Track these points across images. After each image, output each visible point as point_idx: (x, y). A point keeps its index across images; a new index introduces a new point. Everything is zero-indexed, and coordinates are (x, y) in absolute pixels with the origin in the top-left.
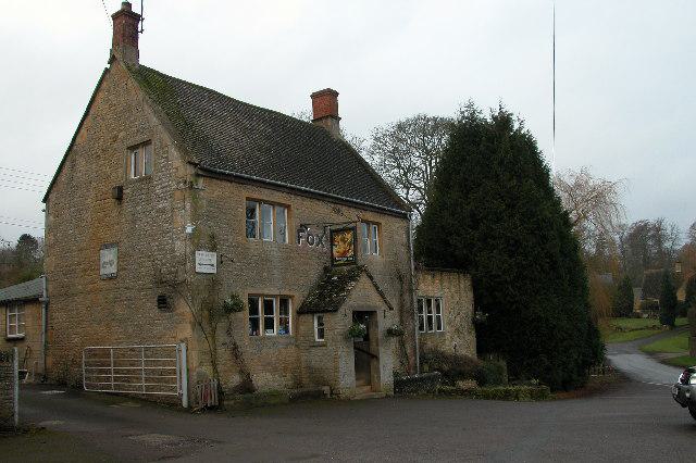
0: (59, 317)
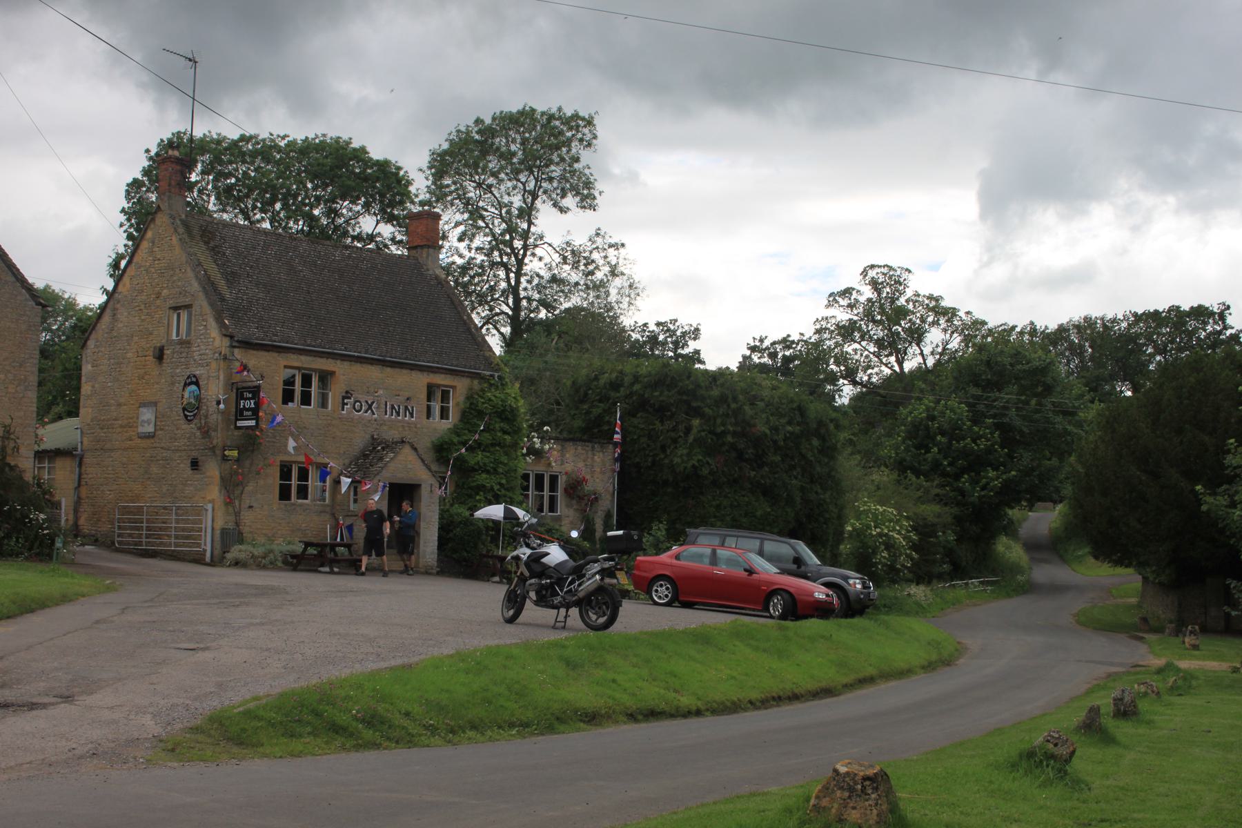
0: (91, 471)
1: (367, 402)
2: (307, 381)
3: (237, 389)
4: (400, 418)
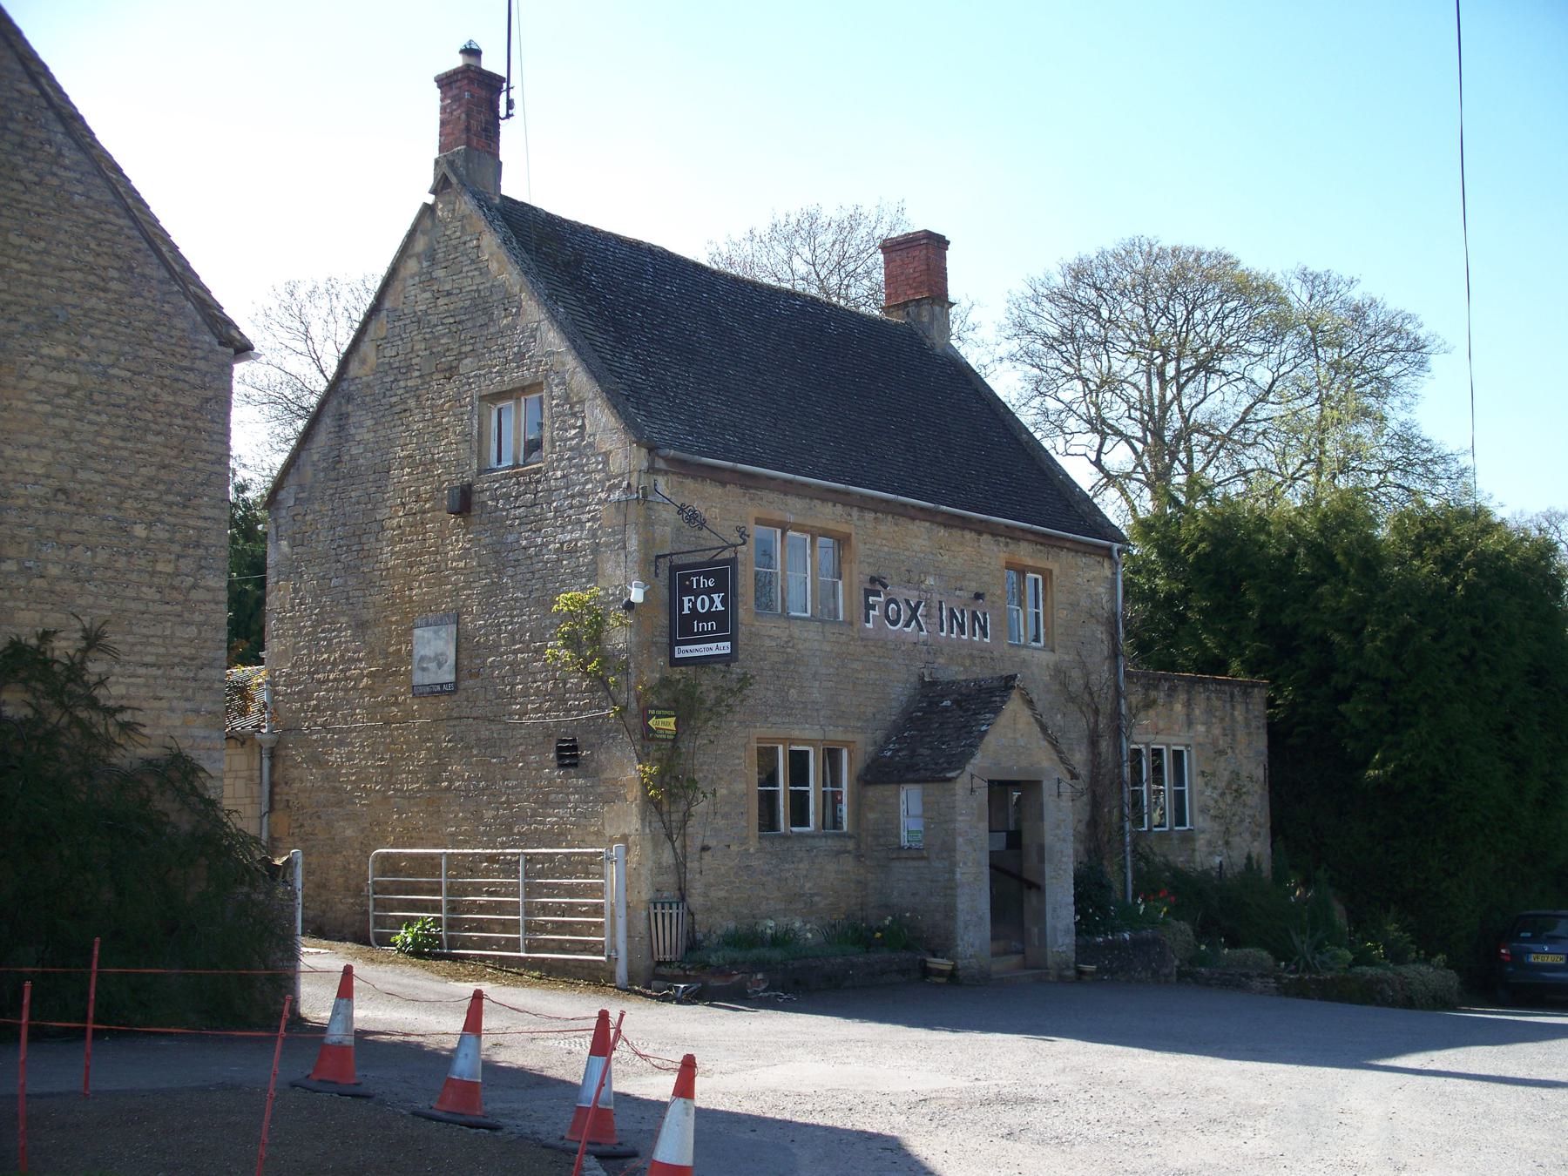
1: (907, 602)
3: (673, 569)
4: (965, 637)
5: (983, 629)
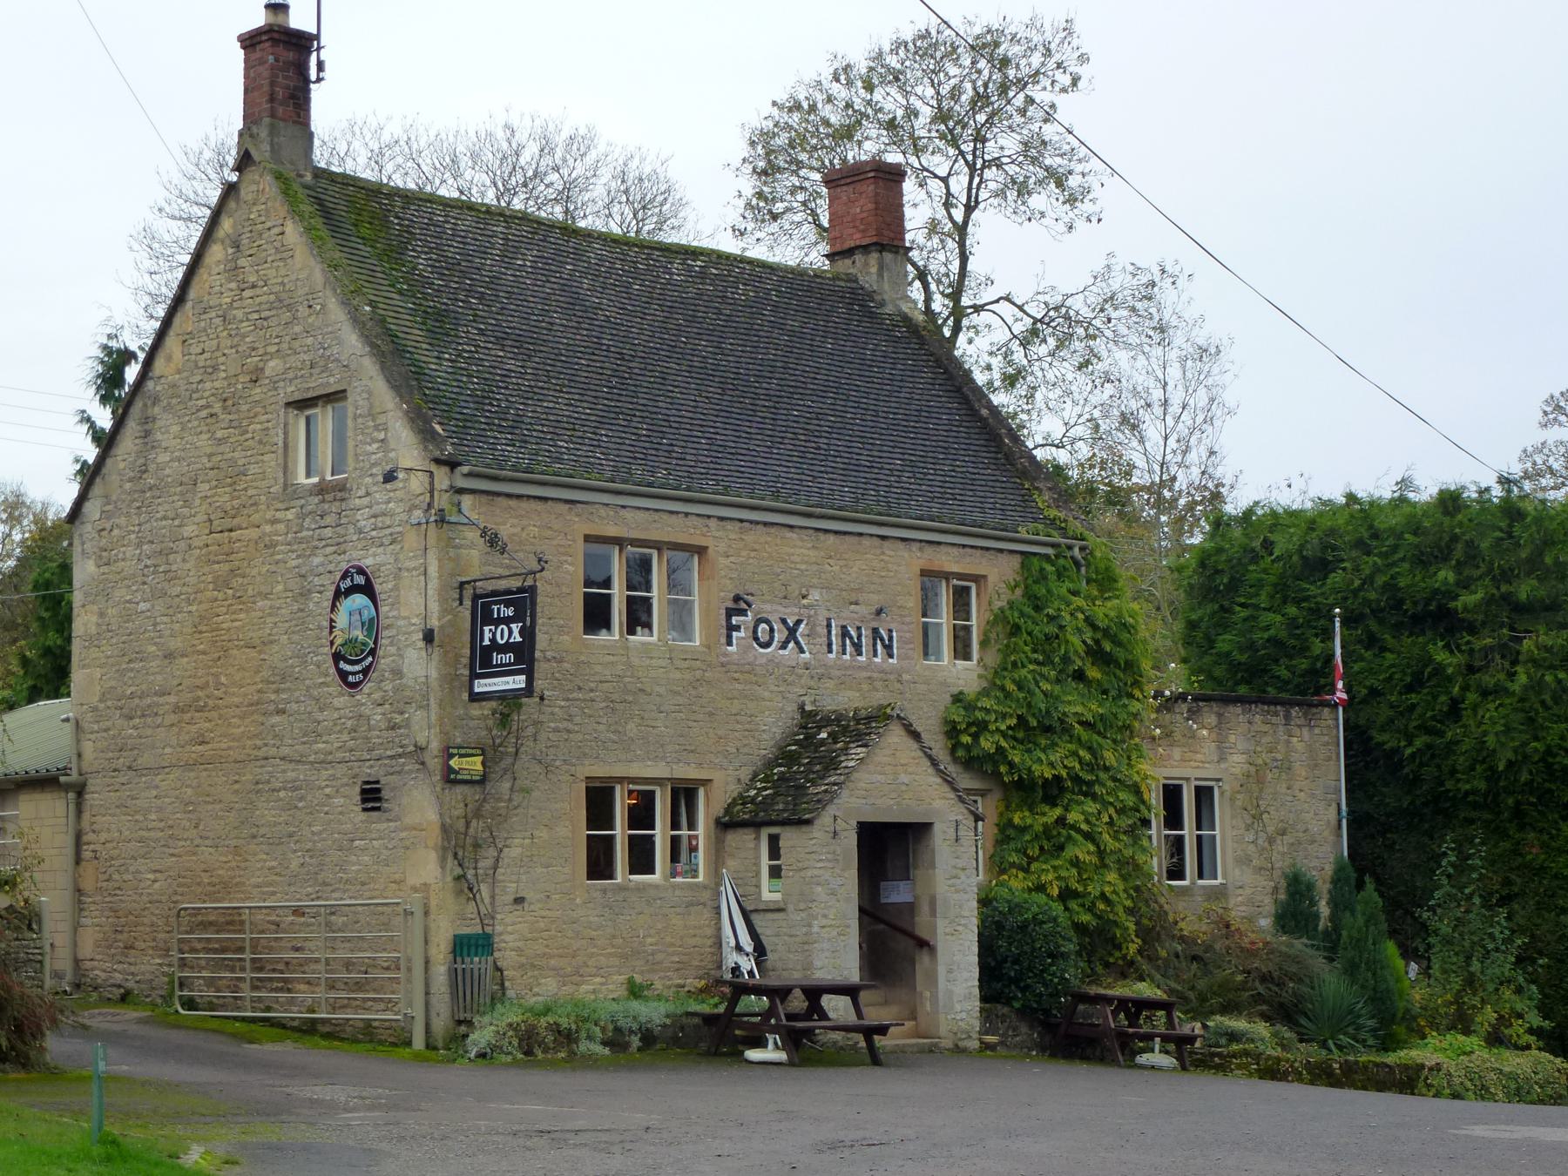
1: (784, 621)
2: (640, 573)
3: (476, 597)
4: (862, 659)
5: (888, 648)
